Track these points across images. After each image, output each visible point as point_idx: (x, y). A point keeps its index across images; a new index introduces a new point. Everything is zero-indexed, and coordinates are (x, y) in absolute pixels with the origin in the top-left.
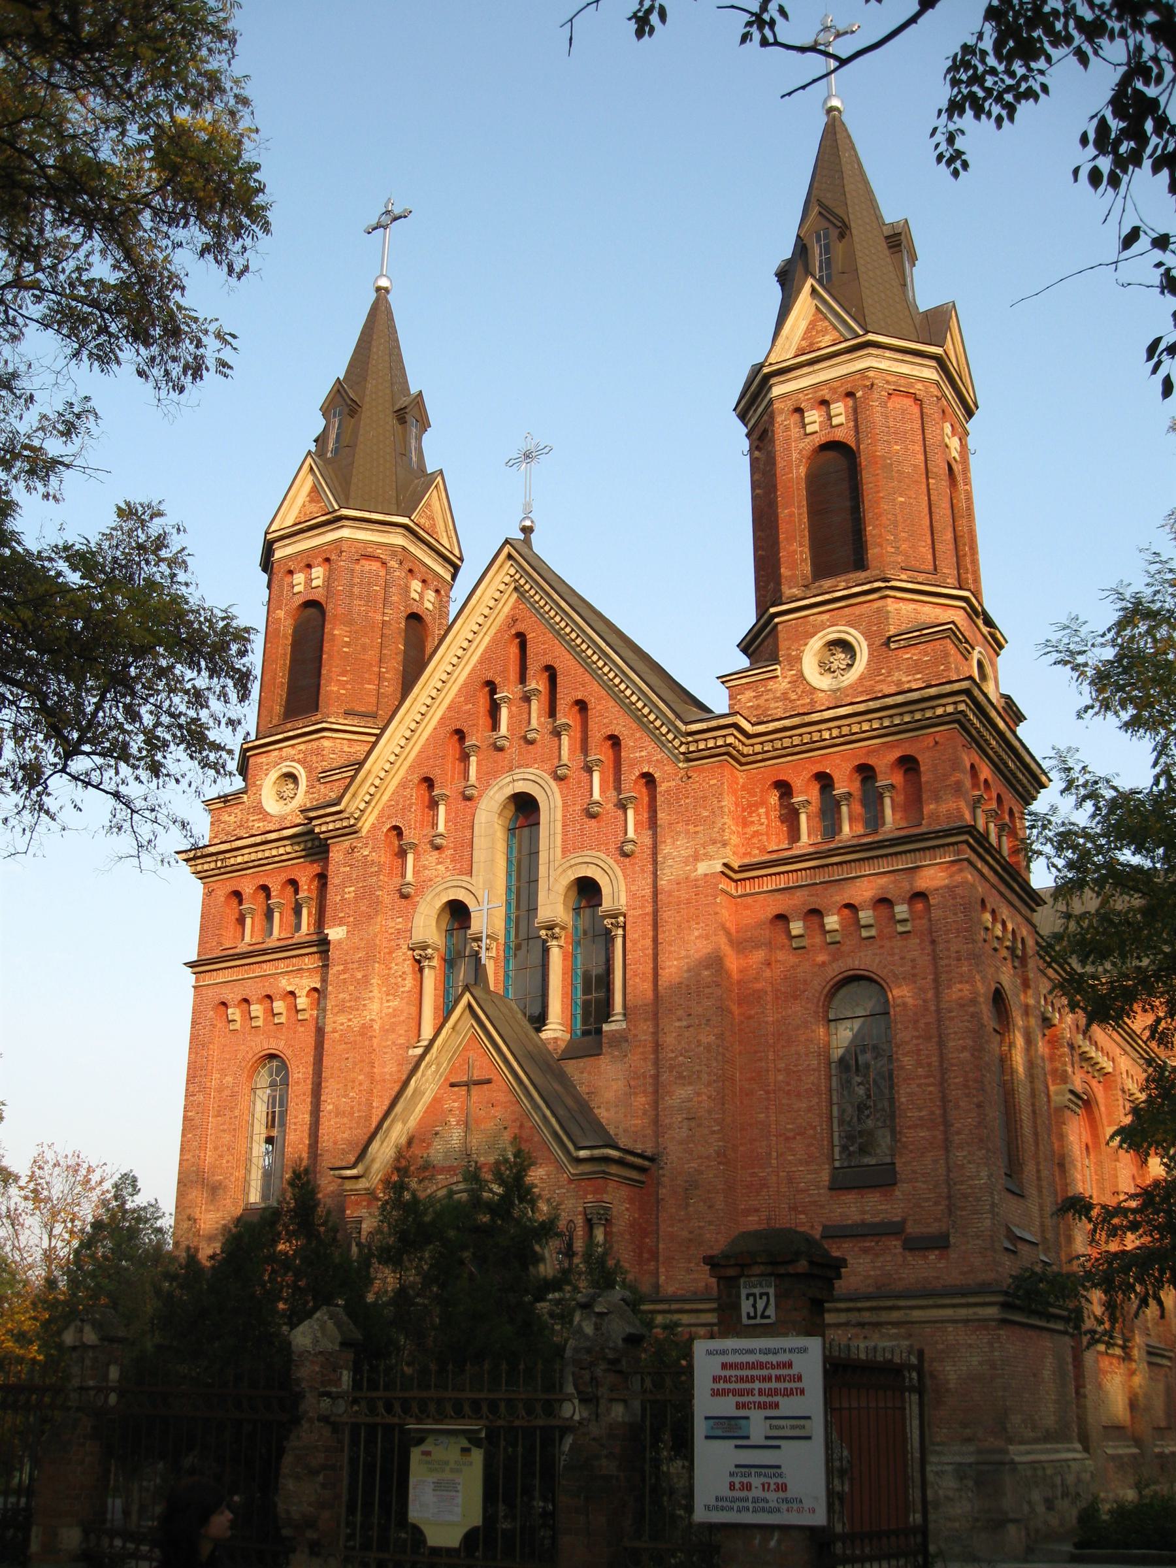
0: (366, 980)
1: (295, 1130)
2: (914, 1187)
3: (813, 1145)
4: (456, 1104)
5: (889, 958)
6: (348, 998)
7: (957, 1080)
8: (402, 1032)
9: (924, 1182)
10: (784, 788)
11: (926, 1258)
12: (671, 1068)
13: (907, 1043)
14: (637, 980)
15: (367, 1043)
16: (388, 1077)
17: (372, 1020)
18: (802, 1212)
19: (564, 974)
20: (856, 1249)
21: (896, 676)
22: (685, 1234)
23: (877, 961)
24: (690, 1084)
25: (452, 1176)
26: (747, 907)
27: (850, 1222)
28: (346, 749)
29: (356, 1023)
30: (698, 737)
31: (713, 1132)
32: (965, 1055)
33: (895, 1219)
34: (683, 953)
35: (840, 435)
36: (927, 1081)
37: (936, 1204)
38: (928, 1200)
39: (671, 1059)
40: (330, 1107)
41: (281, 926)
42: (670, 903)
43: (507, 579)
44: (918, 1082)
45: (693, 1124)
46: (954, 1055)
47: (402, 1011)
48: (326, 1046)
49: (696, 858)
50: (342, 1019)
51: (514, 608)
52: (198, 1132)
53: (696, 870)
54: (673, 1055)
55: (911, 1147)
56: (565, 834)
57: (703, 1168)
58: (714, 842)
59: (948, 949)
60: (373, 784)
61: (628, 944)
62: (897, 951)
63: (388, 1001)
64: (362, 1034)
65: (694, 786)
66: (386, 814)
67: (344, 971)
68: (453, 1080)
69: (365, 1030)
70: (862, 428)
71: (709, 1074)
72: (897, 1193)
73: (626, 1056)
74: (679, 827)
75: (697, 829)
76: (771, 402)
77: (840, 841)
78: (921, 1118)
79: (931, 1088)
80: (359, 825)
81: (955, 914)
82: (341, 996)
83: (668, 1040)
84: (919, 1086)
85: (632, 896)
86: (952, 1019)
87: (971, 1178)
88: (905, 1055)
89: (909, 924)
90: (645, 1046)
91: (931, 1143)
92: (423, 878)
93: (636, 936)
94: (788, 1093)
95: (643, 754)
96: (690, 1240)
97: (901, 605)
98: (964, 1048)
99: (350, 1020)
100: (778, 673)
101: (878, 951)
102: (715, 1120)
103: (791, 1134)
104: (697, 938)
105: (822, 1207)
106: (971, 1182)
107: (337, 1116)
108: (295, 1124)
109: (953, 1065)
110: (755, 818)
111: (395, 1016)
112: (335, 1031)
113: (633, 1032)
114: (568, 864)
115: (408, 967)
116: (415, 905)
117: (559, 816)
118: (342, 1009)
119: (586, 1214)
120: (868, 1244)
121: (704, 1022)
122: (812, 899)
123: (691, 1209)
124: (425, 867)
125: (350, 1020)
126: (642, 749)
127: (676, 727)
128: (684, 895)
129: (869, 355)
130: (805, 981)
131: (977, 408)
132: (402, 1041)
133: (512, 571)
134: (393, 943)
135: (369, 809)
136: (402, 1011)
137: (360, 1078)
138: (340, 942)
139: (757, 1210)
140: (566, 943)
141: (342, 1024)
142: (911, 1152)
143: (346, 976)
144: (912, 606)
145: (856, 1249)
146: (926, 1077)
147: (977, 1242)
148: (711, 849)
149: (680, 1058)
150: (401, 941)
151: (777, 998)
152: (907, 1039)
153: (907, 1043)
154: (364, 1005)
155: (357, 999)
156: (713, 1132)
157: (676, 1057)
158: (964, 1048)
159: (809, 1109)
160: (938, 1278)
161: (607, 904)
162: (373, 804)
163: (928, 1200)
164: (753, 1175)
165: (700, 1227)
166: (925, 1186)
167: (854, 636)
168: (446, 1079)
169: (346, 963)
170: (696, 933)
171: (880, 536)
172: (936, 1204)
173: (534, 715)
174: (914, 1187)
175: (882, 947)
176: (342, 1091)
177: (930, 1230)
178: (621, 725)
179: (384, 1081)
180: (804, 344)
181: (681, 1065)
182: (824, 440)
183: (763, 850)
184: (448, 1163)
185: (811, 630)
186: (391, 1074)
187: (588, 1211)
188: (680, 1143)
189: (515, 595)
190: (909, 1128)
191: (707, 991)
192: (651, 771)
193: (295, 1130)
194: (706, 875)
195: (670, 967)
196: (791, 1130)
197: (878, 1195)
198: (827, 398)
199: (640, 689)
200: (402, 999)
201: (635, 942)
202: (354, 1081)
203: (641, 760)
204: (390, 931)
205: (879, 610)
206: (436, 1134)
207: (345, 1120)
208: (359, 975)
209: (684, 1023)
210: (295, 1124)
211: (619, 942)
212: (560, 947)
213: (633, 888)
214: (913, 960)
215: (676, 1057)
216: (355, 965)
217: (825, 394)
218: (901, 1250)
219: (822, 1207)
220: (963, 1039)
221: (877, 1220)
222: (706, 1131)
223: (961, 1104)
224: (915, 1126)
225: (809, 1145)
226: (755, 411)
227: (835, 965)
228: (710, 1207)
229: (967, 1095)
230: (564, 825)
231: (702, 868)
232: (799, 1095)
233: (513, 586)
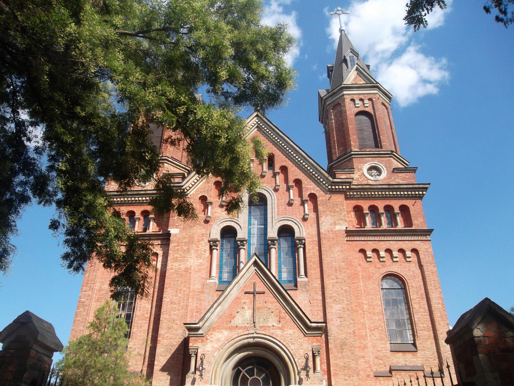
0: (188, 250)
1: (140, 310)
2: (425, 353)
3: (382, 333)
4: (247, 301)
5: (404, 269)
6: (179, 256)
7: (438, 314)
8: (204, 272)
9: (428, 351)
10: (358, 210)
12: (331, 297)
13: (415, 299)
14: (311, 264)
15: (188, 275)
16: (196, 290)
17: (190, 266)
18: (381, 359)
19: (276, 259)
20: (407, 375)
21: (397, 180)
22: (342, 364)
23: (400, 270)
24: (339, 304)
25: (245, 331)
26: (349, 245)
27: (400, 365)
28: (172, 169)
29: (183, 267)
30: (336, 184)
31: (351, 324)
32: (440, 306)
33: (419, 365)
34: (332, 256)
35: (367, 109)
37: (434, 360)
38: (431, 358)
39: (331, 294)
40: (168, 300)
41: (138, 228)
42: (325, 238)
43: (255, 123)
44: (421, 314)
45: (342, 320)
46: (436, 305)
47: (204, 265)
48: (167, 275)
49: (335, 224)
50: (176, 264)
51: (255, 133)
52: (87, 308)
53: (335, 228)
54: (331, 292)
55: (421, 338)
56: (278, 209)
57: (348, 337)
58: (342, 220)
59: (428, 269)
60: (196, 179)
61: (307, 250)
62: (407, 267)
63: (197, 260)
64: (186, 271)
65: (332, 200)
66: (200, 191)
67: (178, 246)
68: (245, 291)
69: (187, 270)
70: (376, 109)
71: (347, 301)
72: (418, 355)
73: (308, 291)
74: (328, 213)
75: (334, 214)
76: (343, 95)
77: (383, 228)
78: (424, 327)
79: (426, 317)
80: (188, 192)
81: (429, 257)
82: (176, 255)
83: (328, 286)
84: (421, 315)
85: (308, 234)
86: (433, 293)
88: (415, 303)
90: (316, 288)
91: (429, 337)
92: (215, 216)
93: (310, 248)
94: (370, 313)
95: (311, 187)
96: (345, 367)
97: (394, 160)
98: (439, 303)
99: (180, 265)
100: (355, 172)
101: (400, 266)
102: (351, 319)
103: (373, 328)
104: (337, 251)
107: (172, 303)
108: (140, 308)
109: (435, 309)
110: (349, 216)
111: (200, 266)
112: (172, 269)
113: (311, 282)
114: (280, 219)
115: (207, 248)
116: (211, 225)
117: (276, 202)
118: (176, 260)
119: (313, 352)
120: (412, 374)
121: (343, 281)
122: (375, 245)
123: (344, 354)
124: (216, 212)
125: (180, 265)
126: (310, 185)
127: (328, 179)
128: (331, 236)
129: (376, 90)
130: (373, 273)
132: (203, 276)
133: (257, 121)
134: (200, 238)
135: (193, 188)
136: (204, 265)
137: (185, 289)
138: (176, 235)
139: (363, 357)
141: (176, 266)
142: (422, 339)
143: (178, 248)
144: (397, 162)
145: (407, 375)
146: (424, 312)
148: (341, 222)
149: (335, 294)
150: (204, 238)
151: (362, 278)
152: (415, 298)
153: (415, 299)
154: (187, 260)
155: (184, 257)
156: (351, 324)
157: (332, 293)
158: (439, 303)
159: (379, 320)
161: (297, 235)
162: (195, 186)
163: (431, 358)
164: (360, 343)
165: (348, 361)
166: (429, 353)
167: (381, 166)
168: (243, 290)
169: (178, 243)
170: (337, 249)
171: (385, 140)
172: (434, 360)
173: (264, 167)
174: (425, 353)
175: (401, 265)
176: (174, 294)
178: (302, 176)
179: (194, 291)
180: (354, 82)
181: (334, 297)
182: (361, 110)
183: (353, 226)
184: (244, 325)
185: (365, 162)
186: (198, 289)
187: (314, 350)
188: (337, 326)
189: (256, 129)
190: (420, 330)
191: (343, 270)
192: (315, 193)
193: (140, 310)
194: (339, 230)
195: (327, 260)
196: (372, 327)
197: (411, 355)
198: (363, 98)
199: (312, 165)
200: (204, 260)
201: (310, 250)
202: (181, 290)
203: (310, 189)
204: (199, 233)
205: (389, 160)
206: (238, 312)
207: (176, 306)
208: (185, 248)
209: (335, 281)
210: (140, 308)
211: (301, 250)
213: (307, 231)
214: (413, 271)
215: (332, 293)
216: (183, 244)
219: (388, 358)
220: (438, 300)
221: (412, 365)
222: (348, 323)
223: (441, 323)
224: (422, 330)
225: (381, 333)
226: (332, 98)
227: (384, 269)
228: (352, 353)
229: (443, 320)
230: (278, 206)
231: (338, 228)
232: (374, 314)
233: (256, 125)
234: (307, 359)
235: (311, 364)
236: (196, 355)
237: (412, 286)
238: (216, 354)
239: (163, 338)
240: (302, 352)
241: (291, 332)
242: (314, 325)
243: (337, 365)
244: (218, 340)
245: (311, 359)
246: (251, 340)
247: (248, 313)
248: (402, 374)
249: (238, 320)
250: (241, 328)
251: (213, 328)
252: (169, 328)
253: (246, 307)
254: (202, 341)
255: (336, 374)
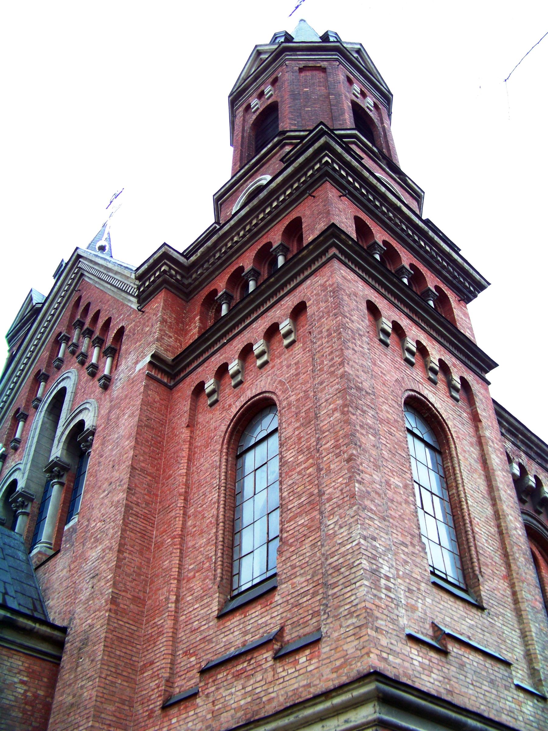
11: (297, 662)
13: (290, 438)
18: (192, 655)
20: (230, 677)
36: (306, 465)
84: (299, 473)
87: (342, 544)
89: (293, 335)
105: (210, 641)
106: (343, 549)
131: (392, 95)
140: (69, 481)
147: (350, 622)
160: (309, 685)
166: (303, 579)
177: (307, 630)
212: (61, 484)
218: (271, 663)
237: (289, 404)
248: (220, 676)
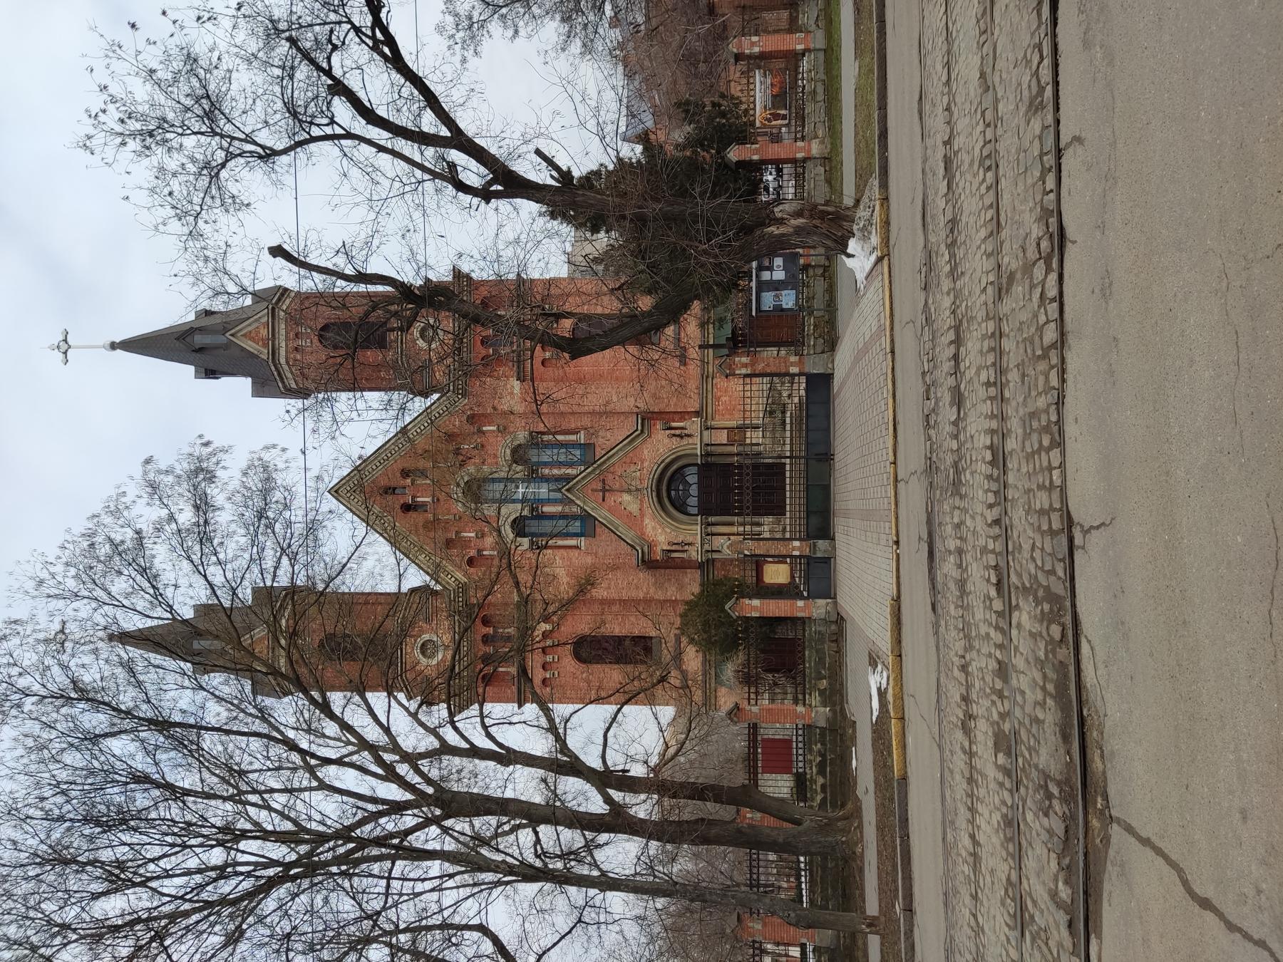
49: (512, 393)
217: (292, 335)
234: (674, 435)
235: (678, 432)
236: (669, 551)
238: (669, 531)
239: (648, 593)
240: (666, 441)
241: (646, 452)
242: (639, 428)
243: (675, 405)
244: (654, 528)
245: (673, 432)
246: (654, 494)
247: (626, 497)
249: (634, 508)
250: (641, 504)
251: (642, 537)
252: (637, 588)
253: (620, 500)
254: (656, 546)
255: (685, 406)
